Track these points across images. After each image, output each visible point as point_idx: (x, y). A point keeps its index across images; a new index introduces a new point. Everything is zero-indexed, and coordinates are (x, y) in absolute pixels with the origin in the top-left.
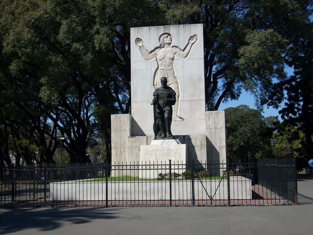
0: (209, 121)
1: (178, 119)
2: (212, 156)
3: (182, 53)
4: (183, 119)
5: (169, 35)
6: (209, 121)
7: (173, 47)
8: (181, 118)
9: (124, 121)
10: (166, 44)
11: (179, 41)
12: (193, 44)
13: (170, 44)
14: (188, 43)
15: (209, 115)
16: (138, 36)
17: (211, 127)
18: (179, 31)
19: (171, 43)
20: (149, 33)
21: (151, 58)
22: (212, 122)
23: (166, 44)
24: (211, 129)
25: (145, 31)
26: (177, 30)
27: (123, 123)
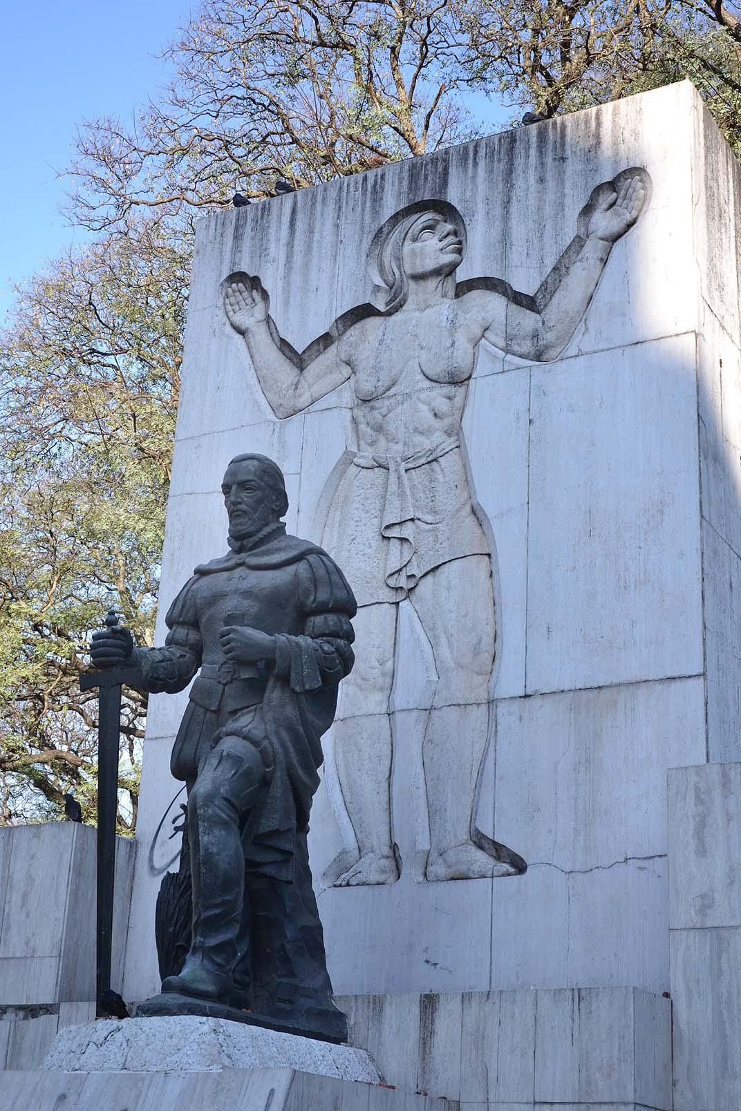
0: (702, 851)
1: (482, 860)
3: (528, 320)
4: (520, 866)
5: (445, 210)
6: (702, 851)
7: (463, 288)
8: (499, 851)
9: (30, 879)
10: (419, 277)
11: (505, 239)
14: (579, 242)
15: (699, 800)
16: (234, 264)
20: (311, 231)
21: (305, 398)
23: (419, 277)
25: (286, 219)
26: (500, 167)
27: (25, 896)
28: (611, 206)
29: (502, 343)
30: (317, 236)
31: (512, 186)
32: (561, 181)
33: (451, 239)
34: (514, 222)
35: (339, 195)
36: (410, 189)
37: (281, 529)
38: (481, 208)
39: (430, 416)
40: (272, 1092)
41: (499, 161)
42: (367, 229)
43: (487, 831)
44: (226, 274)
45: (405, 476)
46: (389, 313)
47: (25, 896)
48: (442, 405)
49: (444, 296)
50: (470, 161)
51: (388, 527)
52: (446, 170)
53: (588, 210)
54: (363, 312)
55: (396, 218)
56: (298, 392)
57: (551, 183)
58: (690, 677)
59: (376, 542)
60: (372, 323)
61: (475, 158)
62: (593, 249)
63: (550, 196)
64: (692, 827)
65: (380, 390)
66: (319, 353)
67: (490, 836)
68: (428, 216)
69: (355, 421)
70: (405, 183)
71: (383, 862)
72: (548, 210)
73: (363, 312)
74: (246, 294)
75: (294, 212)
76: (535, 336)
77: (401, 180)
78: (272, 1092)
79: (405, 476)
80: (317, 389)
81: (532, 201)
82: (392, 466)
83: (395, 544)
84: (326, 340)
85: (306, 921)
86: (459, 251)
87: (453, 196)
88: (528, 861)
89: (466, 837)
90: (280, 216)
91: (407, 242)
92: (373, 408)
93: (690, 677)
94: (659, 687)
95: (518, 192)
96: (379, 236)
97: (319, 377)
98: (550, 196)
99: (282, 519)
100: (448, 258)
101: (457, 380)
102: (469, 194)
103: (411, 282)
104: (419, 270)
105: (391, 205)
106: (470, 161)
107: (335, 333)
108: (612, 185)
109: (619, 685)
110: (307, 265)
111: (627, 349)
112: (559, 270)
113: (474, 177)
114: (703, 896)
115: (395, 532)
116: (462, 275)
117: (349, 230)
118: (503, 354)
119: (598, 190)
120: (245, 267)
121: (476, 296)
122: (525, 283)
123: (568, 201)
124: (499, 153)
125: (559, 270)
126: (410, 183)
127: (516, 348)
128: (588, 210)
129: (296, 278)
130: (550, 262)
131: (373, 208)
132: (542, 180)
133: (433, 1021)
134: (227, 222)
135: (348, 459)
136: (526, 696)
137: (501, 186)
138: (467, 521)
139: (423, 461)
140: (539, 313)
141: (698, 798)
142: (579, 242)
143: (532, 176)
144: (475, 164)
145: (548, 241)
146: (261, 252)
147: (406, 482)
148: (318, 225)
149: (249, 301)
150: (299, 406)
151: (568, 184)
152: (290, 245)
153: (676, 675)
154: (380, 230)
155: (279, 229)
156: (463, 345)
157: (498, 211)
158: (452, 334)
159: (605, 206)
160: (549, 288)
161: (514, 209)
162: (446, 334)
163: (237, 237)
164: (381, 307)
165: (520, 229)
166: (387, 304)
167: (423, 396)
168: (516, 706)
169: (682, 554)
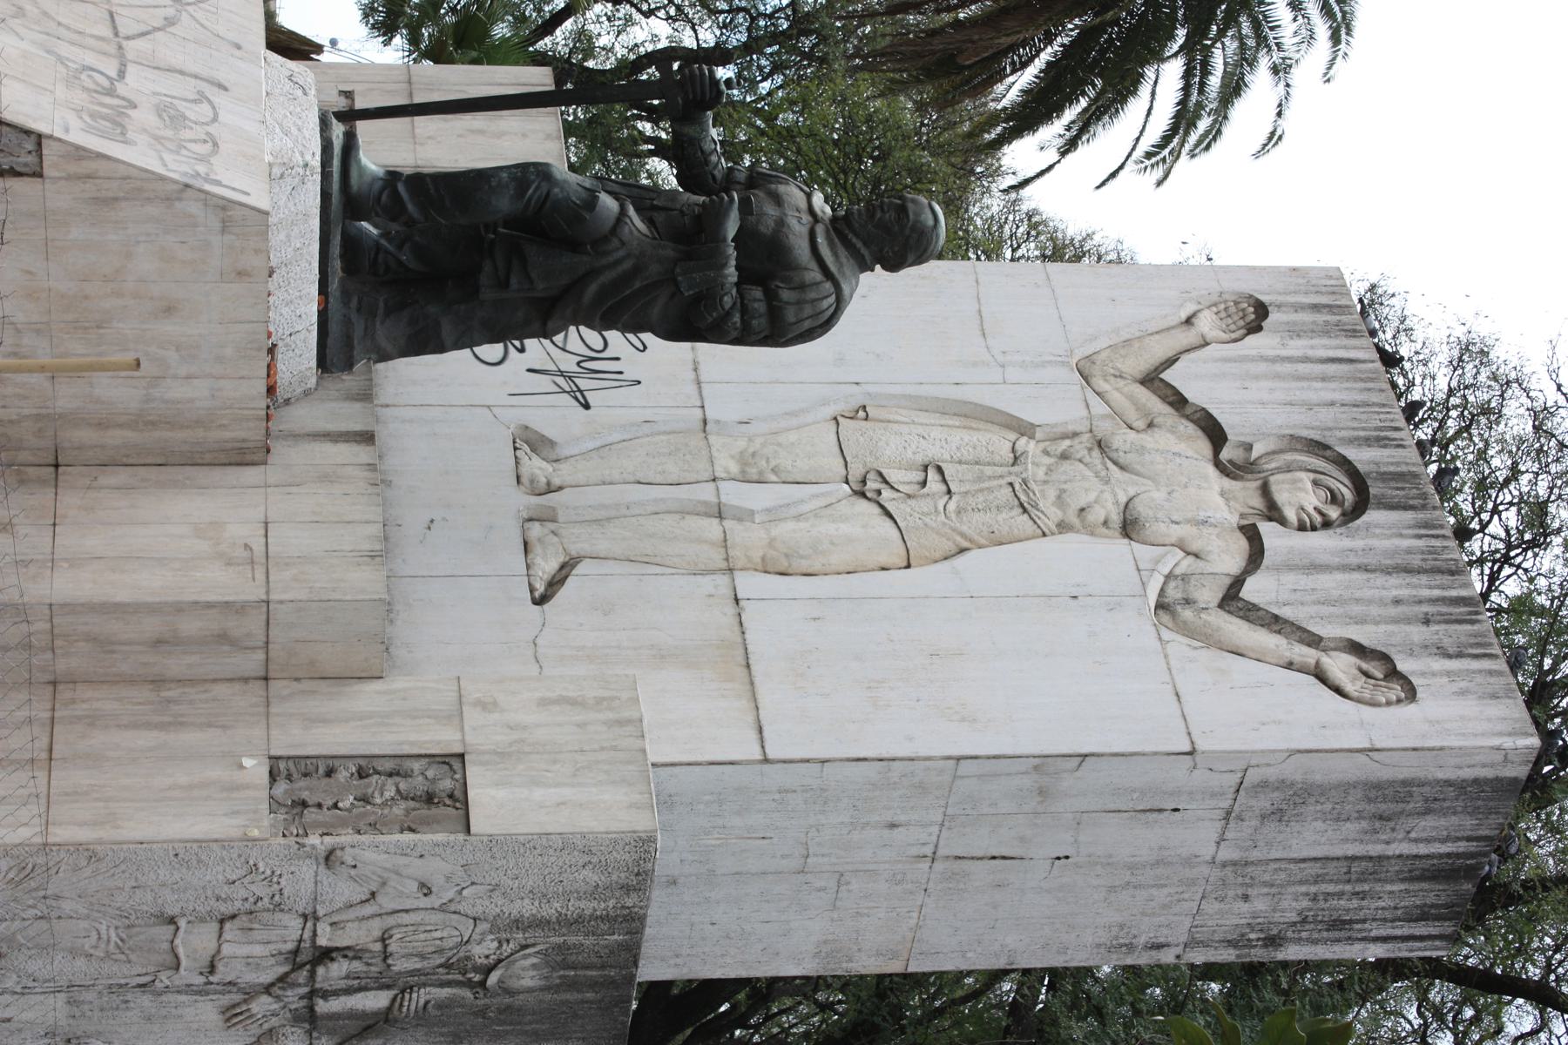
0: (544, 703)
1: (547, 566)
2: (149, 726)
3: (1209, 595)
6: (544, 703)
7: (1252, 534)
8: (555, 583)
9: (500, 135)
10: (1265, 490)
12: (1321, 676)
13: (1273, 512)
14: (1314, 641)
15: (599, 701)
16: (1279, 306)
17: (472, 716)
18: (1408, 570)
19: (1282, 521)
22: (525, 728)
23: (1265, 490)
24: (457, 715)
26: (1416, 561)
27: (481, 132)
28: (1366, 674)
29: (1178, 571)
30: (1319, 385)
31: (1389, 573)
32: (1396, 621)
33: (1318, 519)
34: (1339, 576)
35: (1374, 404)
36: (1385, 473)
37: (866, 267)
38: (1359, 543)
39: (1082, 504)
40: (248, 194)
41: (1423, 560)
42: (1328, 433)
43: (579, 570)
44: (1264, 298)
45: (1003, 482)
46: (1218, 464)
47: (481, 132)
48: (1097, 515)
49: (1242, 516)
50: (1423, 532)
51: (940, 470)
52: (1412, 508)
53: (1356, 649)
54: (1215, 433)
55: (1344, 464)
56: (1112, 378)
57: (1393, 611)
58: (763, 747)
59: (920, 459)
60: (1205, 446)
61: (1427, 536)
62: (1308, 655)
63: (1375, 611)
64: (571, 694)
65: (1114, 455)
66: (1163, 398)
67: (574, 572)
68: (1348, 495)
69: (1075, 435)
70: (1392, 469)
71: (544, 480)
72: (1356, 609)
73: (1215, 433)
74: (1242, 323)
75: (1351, 361)
76: (1188, 602)
77: (1397, 464)
78: (248, 194)
79: (1003, 482)
80: (1115, 397)
81: (1368, 593)
82: (1016, 469)
83: (920, 476)
84: (1178, 401)
85: (447, 330)
86: (1302, 528)
87: (1372, 516)
88: (546, 607)
89: (574, 553)
90: (1345, 347)
91: (1312, 476)
92: (1090, 450)
93: (763, 747)
94: (751, 718)
95: (1380, 580)
96: (1318, 447)
97: (1131, 398)
98: (1375, 611)
99: (878, 267)
100: (1291, 515)
101: (1129, 527)
102: (1378, 531)
103: (1259, 483)
104: (1274, 488)
105: (1361, 457)
106: (1423, 532)
107: (1188, 411)
108: (1393, 674)
109: (752, 683)
110: (1278, 377)
111: (1170, 687)
112: (1275, 623)
113: (1401, 535)
114: (495, 704)
115: (932, 475)
116: (1267, 529)
117: (1326, 416)
118: (1166, 571)
119: (1385, 658)
120: (1274, 317)
121: (1242, 544)
122: (1253, 590)
123: (1370, 628)
124: (1436, 560)
125: (1275, 623)
126: (1391, 473)
127: (1172, 584)
128: (1356, 649)
129: (1262, 367)
130: (1286, 612)
131: (1357, 439)
132: (1397, 602)
133: (347, 441)
134: (1338, 297)
135: (1025, 429)
136: (737, 600)
137: (1389, 562)
138: (950, 543)
139: (1023, 498)
140: (1221, 606)
141: (603, 699)
142: (1314, 641)
143: (1404, 593)
144: (1420, 537)
145: (1313, 610)
146: (1295, 332)
147: (995, 483)
148: (1333, 385)
149: (1233, 327)
150: (1094, 381)
151: (1391, 628)
152: (1306, 360)
153: (766, 734)
154: (1326, 447)
155: (1325, 347)
156: (1176, 532)
157: (1353, 560)
158: (1188, 521)
159: (1365, 666)
160: (1252, 614)
161: (1358, 577)
162: (1189, 515)
163: (1316, 308)
164: (1225, 454)
165: (1329, 582)
166: (1230, 461)
167: (1108, 496)
168: (726, 591)
169: (911, 739)
